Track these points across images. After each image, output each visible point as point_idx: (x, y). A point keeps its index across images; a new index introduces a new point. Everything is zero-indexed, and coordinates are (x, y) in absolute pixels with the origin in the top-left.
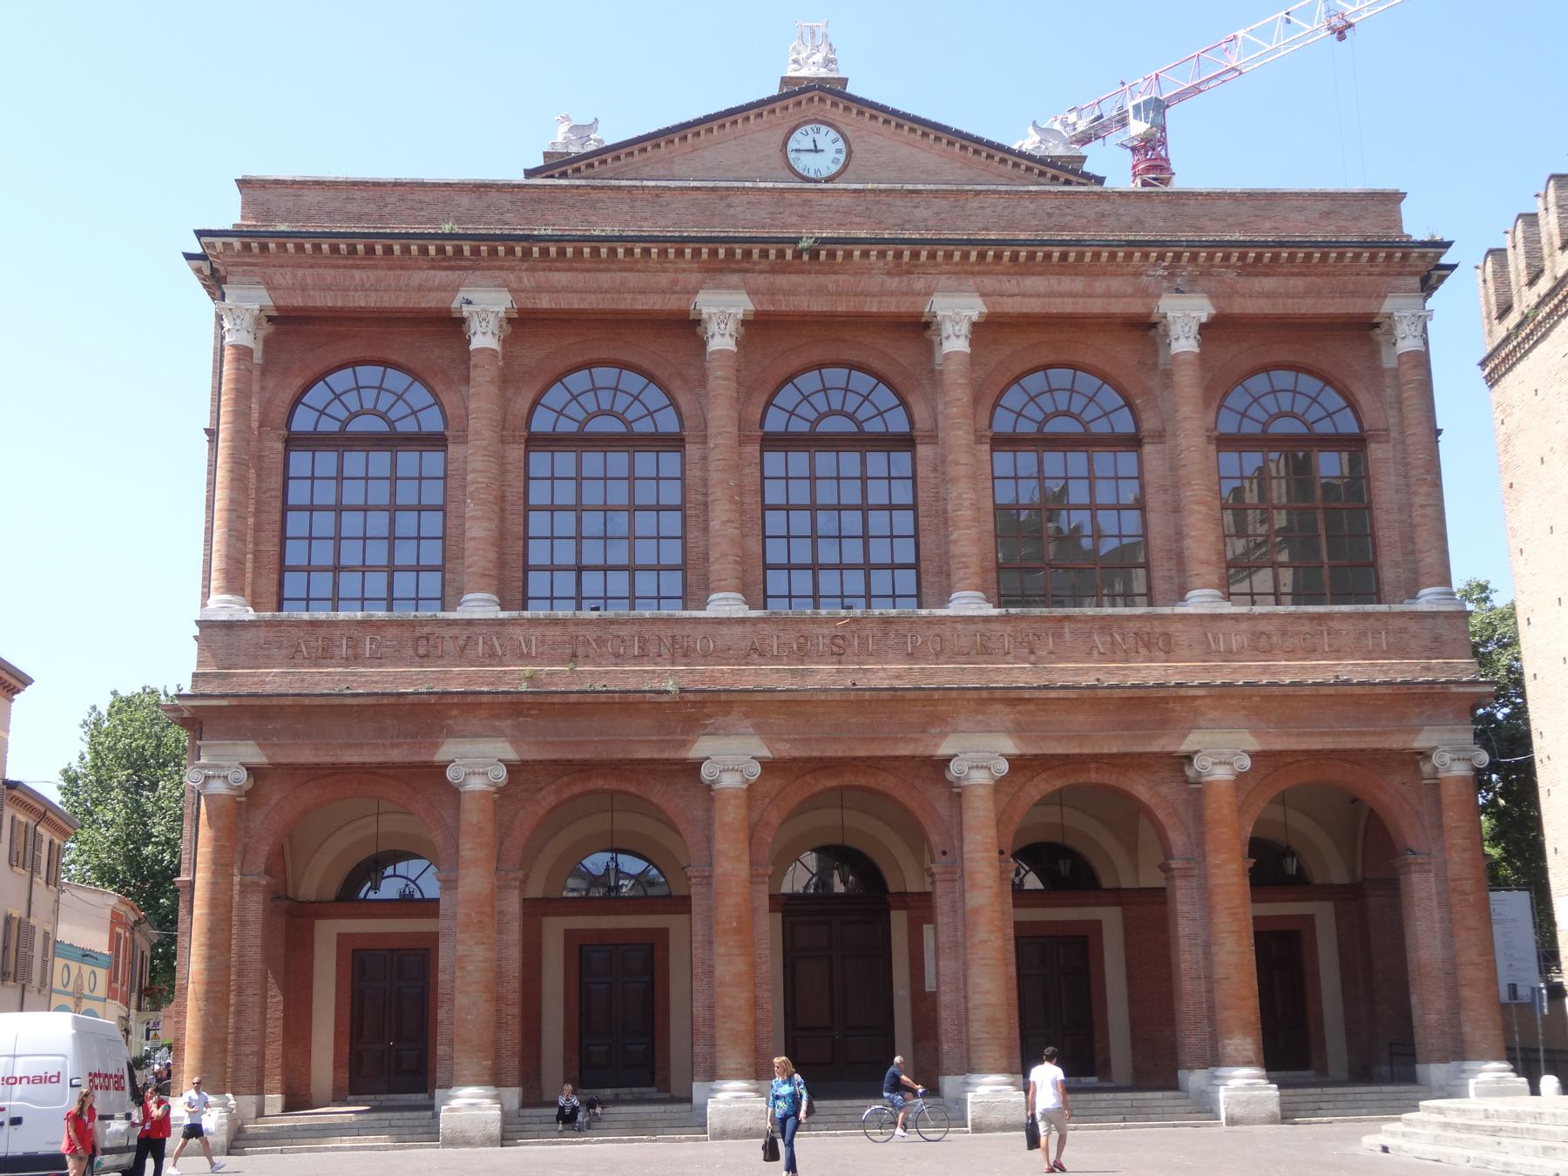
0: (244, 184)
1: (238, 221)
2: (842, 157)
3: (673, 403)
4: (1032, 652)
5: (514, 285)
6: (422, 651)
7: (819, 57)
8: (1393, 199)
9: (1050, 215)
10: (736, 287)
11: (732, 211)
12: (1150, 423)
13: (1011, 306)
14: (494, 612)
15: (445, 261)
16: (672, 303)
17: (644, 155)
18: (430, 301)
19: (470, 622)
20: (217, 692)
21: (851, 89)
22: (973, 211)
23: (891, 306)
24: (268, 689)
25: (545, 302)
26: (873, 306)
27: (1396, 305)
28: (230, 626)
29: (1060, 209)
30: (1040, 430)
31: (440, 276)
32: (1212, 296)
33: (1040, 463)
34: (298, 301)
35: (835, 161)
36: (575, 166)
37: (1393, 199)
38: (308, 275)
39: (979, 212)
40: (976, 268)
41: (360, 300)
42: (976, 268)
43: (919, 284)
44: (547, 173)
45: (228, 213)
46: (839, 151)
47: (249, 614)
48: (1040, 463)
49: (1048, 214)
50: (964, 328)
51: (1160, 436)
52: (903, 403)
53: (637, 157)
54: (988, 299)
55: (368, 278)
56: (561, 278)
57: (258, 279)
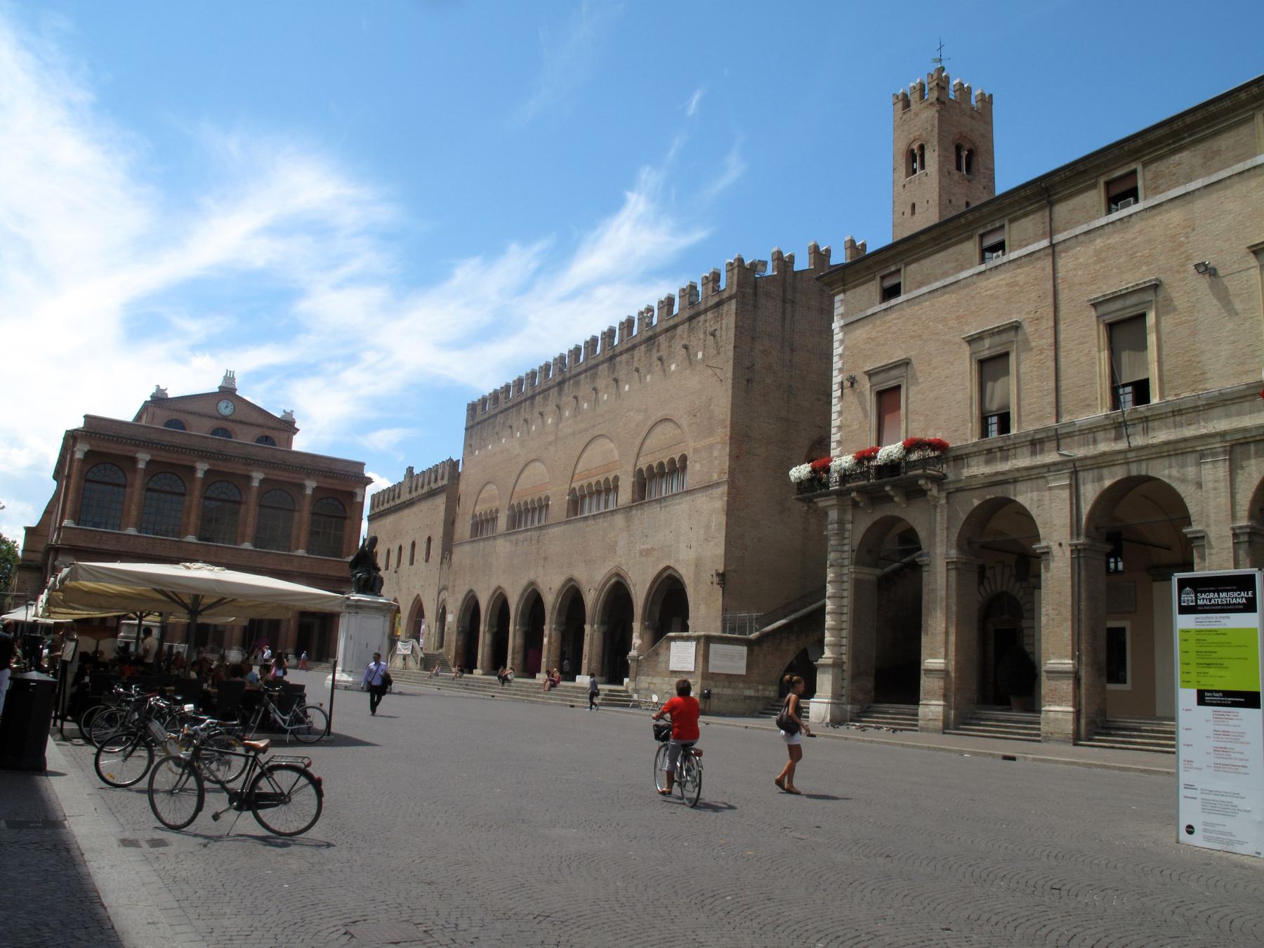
0: (87, 417)
3: (184, 485)
8: (362, 465)
12: (297, 508)
13: (271, 477)
14: (136, 533)
15: (135, 445)
16: (190, 464)
18: (130, 454)
19: (130, 535)
21: (237, 393)
25: (159, 459)
26: (238, 472)
27: (358, 491)
28: (70, 528)
31: (133, 448)
32: (317, 482)
34: (97, 449)
37: (362, 465)
41: (112, 451)
43: (250, 469)
45: (79, 423)
47: (73, 526)
50: (258, 481)
51: (299, 511)
52: (240, 493)
56: (164, 454)
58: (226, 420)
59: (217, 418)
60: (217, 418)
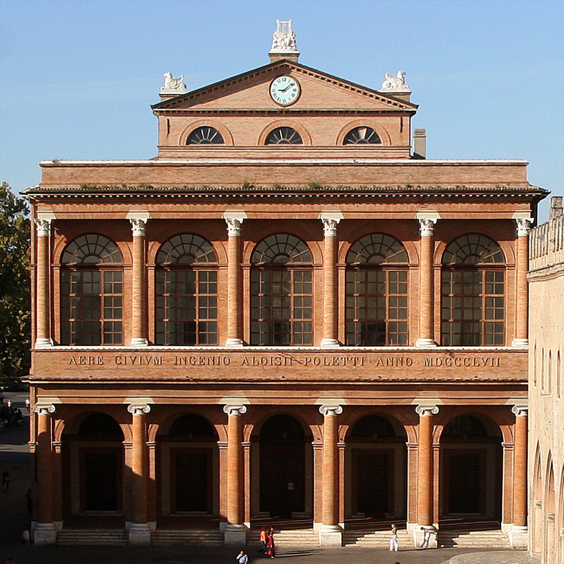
1: (41, 182)
2: (296, 93)
4: (355, 365)
5: (151, 210)
6: (118, 362)
7: (287, 41)
9: (374, 173)
10: (240, 208)
11: (239, 173)
16: (214, 216)
17: (204, 95)
20: (43, 377)
22: (340, 172)
23: (304, 216)
24: (62, 377)
25: (163, 216)
29: (378, 171)
30: (367, 261)
33: (366, 276)
35: (293, 95)
36: (173, 102)
38: (69, 207)
39: (343, 172)
40: (340, 200)
42: (340, 200)
43: (316, 207)
44: (162, 106)
46: (295, 90)
48: (366, 276)
49: (372, 173)
53: (201, 96)
54: (344, 213)
55: (93, 207)
57: (50, 208)
58: (287, 112)
59: (271, 113)
60: (271, 113)
